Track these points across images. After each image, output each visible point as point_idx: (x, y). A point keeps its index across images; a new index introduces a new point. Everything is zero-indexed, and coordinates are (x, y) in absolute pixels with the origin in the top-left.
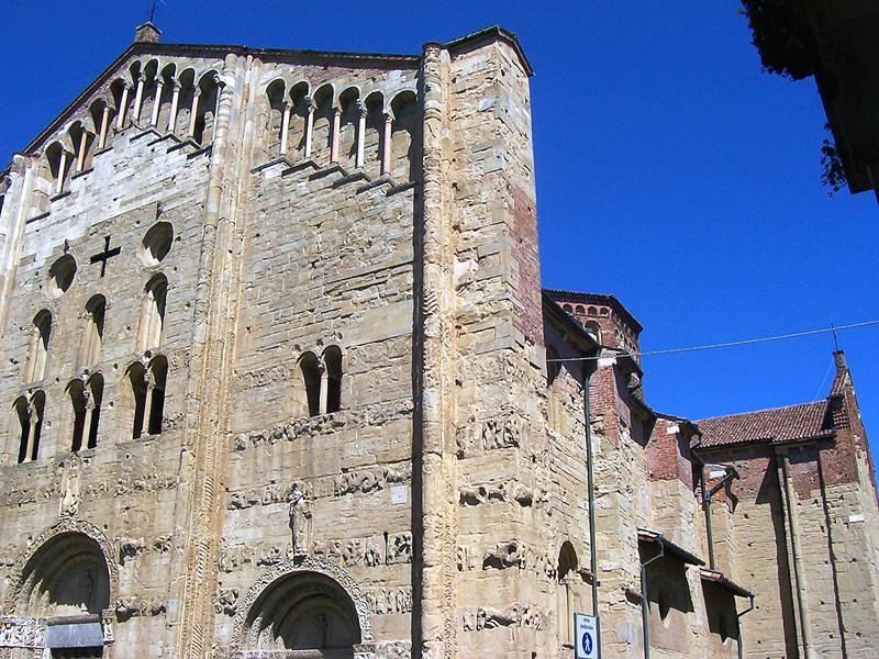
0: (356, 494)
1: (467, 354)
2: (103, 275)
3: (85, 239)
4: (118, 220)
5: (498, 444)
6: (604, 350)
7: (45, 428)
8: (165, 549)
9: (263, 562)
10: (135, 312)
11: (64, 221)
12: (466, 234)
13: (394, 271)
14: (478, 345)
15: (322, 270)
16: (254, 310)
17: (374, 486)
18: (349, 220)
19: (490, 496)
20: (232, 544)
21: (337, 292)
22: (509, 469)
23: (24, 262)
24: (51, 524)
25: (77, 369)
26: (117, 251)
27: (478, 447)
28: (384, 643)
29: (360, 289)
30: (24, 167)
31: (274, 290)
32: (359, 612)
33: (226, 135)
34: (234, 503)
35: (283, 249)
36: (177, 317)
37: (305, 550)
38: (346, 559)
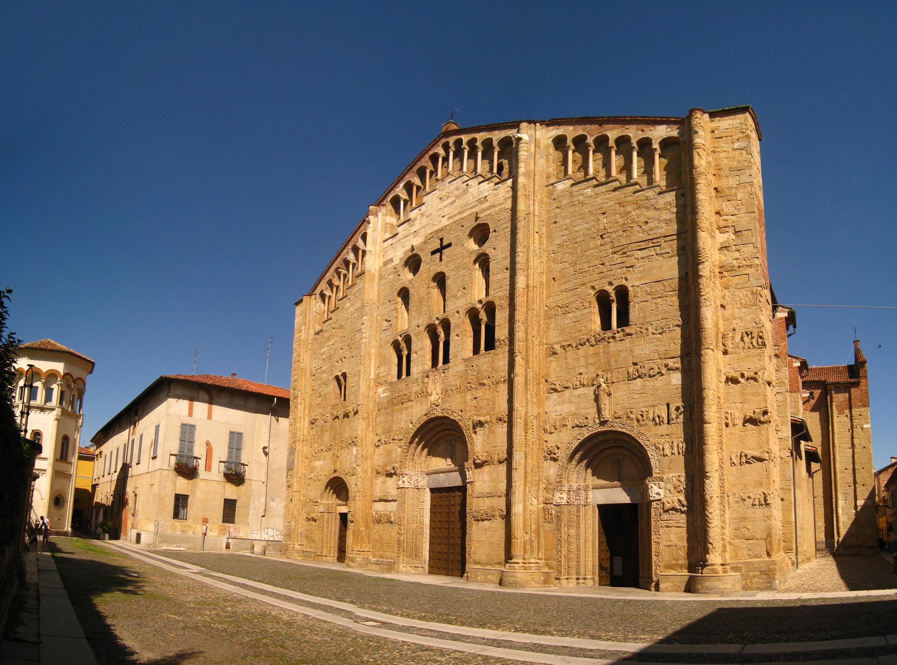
5: (753, 346)
9: (577, 426)
13: (666, 239)
17: (658, 373)
19: (748, 379)
20: (553, 416)
24: (424, 413)
28: (670, 475)
32: (650, 456)
34: (552, 389)
37: (608, 416)
38: (638, 421)
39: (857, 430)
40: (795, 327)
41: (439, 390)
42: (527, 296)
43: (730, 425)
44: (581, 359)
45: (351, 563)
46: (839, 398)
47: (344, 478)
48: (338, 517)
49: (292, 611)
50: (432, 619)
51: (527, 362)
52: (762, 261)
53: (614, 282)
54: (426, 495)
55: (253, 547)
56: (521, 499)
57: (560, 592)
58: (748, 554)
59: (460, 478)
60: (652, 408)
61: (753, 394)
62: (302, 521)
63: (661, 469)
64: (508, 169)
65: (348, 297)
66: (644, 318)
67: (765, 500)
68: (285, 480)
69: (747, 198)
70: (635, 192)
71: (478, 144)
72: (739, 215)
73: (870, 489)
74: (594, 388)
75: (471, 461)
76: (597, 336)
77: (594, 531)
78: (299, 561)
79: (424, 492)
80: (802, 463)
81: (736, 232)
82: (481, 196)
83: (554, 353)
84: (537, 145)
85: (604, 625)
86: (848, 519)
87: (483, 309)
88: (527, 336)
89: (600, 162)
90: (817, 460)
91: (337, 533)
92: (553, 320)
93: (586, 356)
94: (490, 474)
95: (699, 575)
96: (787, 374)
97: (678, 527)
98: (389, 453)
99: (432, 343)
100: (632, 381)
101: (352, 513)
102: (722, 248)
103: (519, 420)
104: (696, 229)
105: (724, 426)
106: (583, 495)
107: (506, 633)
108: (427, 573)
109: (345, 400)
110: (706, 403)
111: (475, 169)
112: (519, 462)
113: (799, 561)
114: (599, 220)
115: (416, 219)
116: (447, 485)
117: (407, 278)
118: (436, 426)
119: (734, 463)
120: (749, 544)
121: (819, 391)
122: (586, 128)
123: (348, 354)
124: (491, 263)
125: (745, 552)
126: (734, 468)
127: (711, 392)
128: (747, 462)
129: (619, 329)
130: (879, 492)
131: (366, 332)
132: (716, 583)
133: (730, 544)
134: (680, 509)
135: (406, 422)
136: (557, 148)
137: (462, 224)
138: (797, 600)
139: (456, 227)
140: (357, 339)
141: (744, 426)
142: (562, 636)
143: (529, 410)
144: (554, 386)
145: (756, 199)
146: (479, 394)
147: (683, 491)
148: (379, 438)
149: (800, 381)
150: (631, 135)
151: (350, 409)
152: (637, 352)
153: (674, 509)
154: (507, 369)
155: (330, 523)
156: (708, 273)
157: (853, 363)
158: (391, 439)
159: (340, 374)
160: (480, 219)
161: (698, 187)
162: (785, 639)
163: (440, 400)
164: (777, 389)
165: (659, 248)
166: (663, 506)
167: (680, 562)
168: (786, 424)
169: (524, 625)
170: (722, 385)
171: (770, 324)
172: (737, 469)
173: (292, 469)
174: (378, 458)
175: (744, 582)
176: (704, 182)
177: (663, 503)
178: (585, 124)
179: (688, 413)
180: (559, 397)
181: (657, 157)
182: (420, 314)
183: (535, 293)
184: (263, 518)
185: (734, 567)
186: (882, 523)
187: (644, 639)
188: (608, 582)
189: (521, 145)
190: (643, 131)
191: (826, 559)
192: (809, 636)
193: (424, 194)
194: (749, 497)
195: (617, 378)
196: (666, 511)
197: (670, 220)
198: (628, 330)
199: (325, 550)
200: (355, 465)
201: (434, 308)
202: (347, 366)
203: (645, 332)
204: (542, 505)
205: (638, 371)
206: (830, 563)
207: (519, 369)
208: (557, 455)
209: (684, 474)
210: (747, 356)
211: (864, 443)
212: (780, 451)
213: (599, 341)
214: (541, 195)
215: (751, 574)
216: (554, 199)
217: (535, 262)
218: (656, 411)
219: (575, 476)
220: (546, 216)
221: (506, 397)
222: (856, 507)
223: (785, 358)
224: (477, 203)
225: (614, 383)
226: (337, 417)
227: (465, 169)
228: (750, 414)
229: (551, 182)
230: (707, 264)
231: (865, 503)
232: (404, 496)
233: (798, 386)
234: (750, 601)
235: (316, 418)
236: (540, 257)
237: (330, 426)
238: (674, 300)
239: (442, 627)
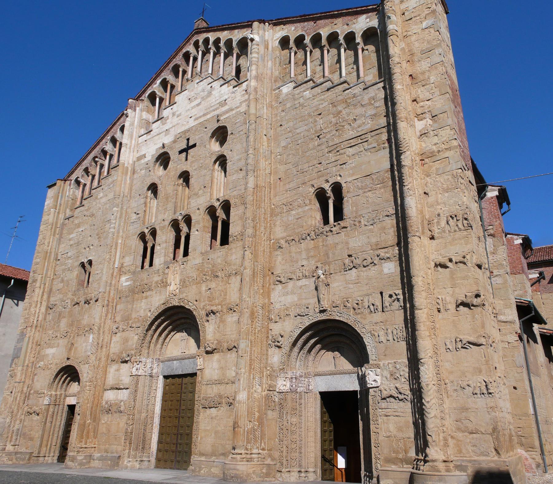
0: (360, 269)
1: (430, 175)
2: (186, 160)
3: (175, 142)
4: (194, 128)
6: (490, 187)
7: (157, 248)
8: (235, 311)
9: (299, 315)
10: (208, 178)
12: (422, 104)
14: (437, 169)
15: (324, 140)
16: (282, 168)
18: (340, 108)
22: (468, 246)
23: (139, 159)
24: (162, 302)
25: (175, 213)
26: (194, 146)
29: (351, 147)
30: (135, 107)
31: (294, 155)
32: (366, 343)
33: (257, 69)
35: (298, 131)
36: (234, 177)
38: (354, 309)
41: (178, 281)
43: (442, 310)
94: (219, 361)
114: (316, 121)
134: (398, 397)
135: (145, 310)
146: (213, 285)
153: (391, 396)
163: (177, 291)
204: (266, 392)
208: (281, 343)
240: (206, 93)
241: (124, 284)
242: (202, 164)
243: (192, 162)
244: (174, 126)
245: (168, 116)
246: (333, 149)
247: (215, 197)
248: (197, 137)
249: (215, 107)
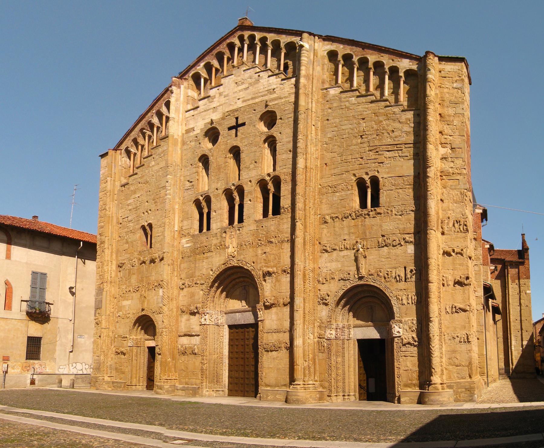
2: (236, 136)
4: (242, 109)
5: (461, 231)
9: (342, 279)
11: (208, 110)
13: (406, 146)
17: (399, 244)
19: (457, 253)
20: (325, 270)
21: (375, 151)
24: (222, 262)
26: (244, 124)
27: (451, 231)
28: (407, 319)
29: (388, 151)
32: (393, 304)
34: (324, 250)
37: (364, 273)
38: (385, 278)
39: (523, 294)
40: (486, 220)
41: (235, 244)
42: (306, 175)
43: (445, 285)
44: (345, 228)
45: (159, 390)
46: (512, 272)
47: (151, 316)
48: (147, 350)
49: (102, 438)
50: (232, 433)
51: (305, 227)
52: (468, 171)
53: (369, 173)
54: (224, 330)
55: (60, 381)
56: (301, 334)
57: (330, 406)
58: (457, 377)
59: (253, 317)
60: (395, 270)
61: (460, 265)
62: (111, 355)
63: (400, 314)
64: (292, 70)
65: (153, 156)
66: (390, 202)
67: (468, 339)
68: (93, 318)
69: (460, 125)
70: (386, 107)
71: (269, 42)
72: (454, 137)
73: (531, 334)
74: (354, 251)
75: (261, 303)
76: (357, 212)
77: (354, 359)
78: (109, 391)
79: (223, 329)
80: (490, 314)
81: (452, 148)
82: (270, 88)
83: (326, 222)
84: (315, 54)
85: (364, 430)
86: (518, 354)
87: (271, 181)
88: (305, 207)
89: (362, 78)
90: (499, 313)
91: (146, 364)
92: (325, 196)
93: (349, 227)
94: (277, 314)
95: (427, 391)
96: (481, 252)
97: (412, 356)
98: (192, 295)
99: (229, 204)
100: (381, 249)
101: (159, 346)
102: (442, 158)
103: (299, 272)
104: (426, 142)
105: (442, 286)
106: (346, 332)
107: (291, 440)
108: (227, 395)
109: (151, 247)
110: (430, 268)
111: (266, 64)
112: (300, 305)
113: (489, 382)
114: (360, 123)
115: (215, 97)
116: (243, 323)
117: (207, 147)
118: (232, 274)
119: (448, 312)
120: (458, 369)
121: (501, 266)
122: (353, 49)
123: (153, 207)
124: (277, 144)
125: (456, 375)
126: (448, 315)
127: (434, 260)
128: (456, 312)
129: (372, 209)
130: (536, 337)
131: (170, 190)
132: (438, 397)
133: (446, 369)
134: (413, 344)
135: (207, 269)
136: (330, 60)
137: (255, 109)
138: (488, 408)
139: (249, 110)
140: (162, 195)
141: (454, 286)
142: (334, 440)
143: (307, 265)
144: (325, 248)
145: (465, 127)
146: (268, 250)
147: (415, 330)
148: (183, 282)
149: (489, 258)
150: (385, 62)
151: (157, 255)
152: (385, 227)
153: (409, 343)
154: (289, 232)
155: (139, 356)
156: (433, 175)
157: (521, 249)
158: (194, 283)
159: (146, 224)
160: (269, 107)
161: (429, 111)
162: (482, 436)
163: (236, 253)
164: (475, 262)
165: (401, 151)
166: (402, 341)
167: (414, 382)
168: (481, 287)
169: (305, 434)
170: (441, 256)
171: (472, 217)
172: (450, 317)
173: (100, 308)
174: (183, 299)
175: (455, 396)
176: (433, 108)
177: (402, 339)
178: (352, 45)
179: (418, 275)
180: (329, 256)
181: (402, 83)
182: (218, 179)
183: (312, 173)
184: (71, 354)
185: (449, 386)
186: (538, 357)
187: (391, 439)
188: (366, 398)
189: (303, 52)
190: (393, 60)
191: (505, 380)
192: (497, 433)
193: (222, 76)
194: (457, 337)
195: (371, 245)
196: (404, 345)
197: (409, 132)
198: (378, 210)
199: (135, 380)
200: (161, 305)
201: (231, 176)
202: (153, 218)
203: (390, 213)
204: (317, 339)
205: (385, 241)
206: (507, 383)
207: (299, 232)
208: (328, 301)
209: (415, 318)
210: (457, 238)
211: (527, 303)
212: (476, 305)
213: (358, 216)
214: (317, 95)
215: (460, 390)
216: (327, 101)
217: (311, 149)
218: (397, 271)
219: (341, 317)
220: (321, 114)
221: (289, 254)
222: (522, 345)
223: (480, 242)
224: (266, 93)
225: (368, 248)
226: (144, 262)
227: (257, 62)
228: (458, 278)
229: (326, 87)
230: (432, 168)
231: (528, 343)
232: (206, 331)
233: (488, 261)
234: (459, 409)
235: (123, 262)
236: (316, 146)
237: (137, 270)
238: (410, 192)
239: (240, 440)
240: (253, 80)
241: (185, 246)
242: (251, 141)
243: (242, 138)
244: (222, 105)
245: (215, 96)
246: (373, 148)
247: (266, 172)
248: (246, 117)
249: (263, 94)
